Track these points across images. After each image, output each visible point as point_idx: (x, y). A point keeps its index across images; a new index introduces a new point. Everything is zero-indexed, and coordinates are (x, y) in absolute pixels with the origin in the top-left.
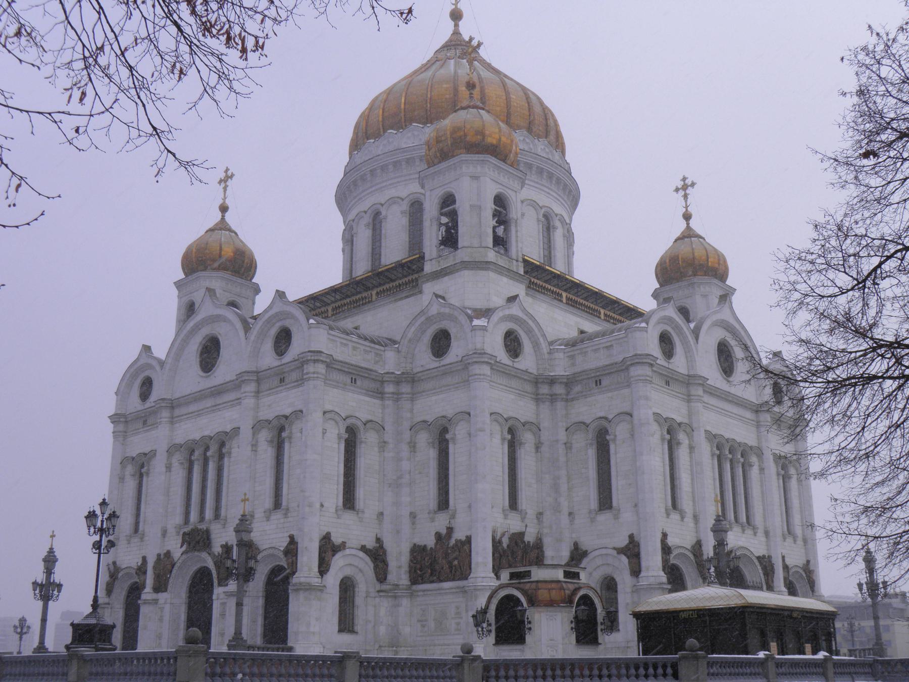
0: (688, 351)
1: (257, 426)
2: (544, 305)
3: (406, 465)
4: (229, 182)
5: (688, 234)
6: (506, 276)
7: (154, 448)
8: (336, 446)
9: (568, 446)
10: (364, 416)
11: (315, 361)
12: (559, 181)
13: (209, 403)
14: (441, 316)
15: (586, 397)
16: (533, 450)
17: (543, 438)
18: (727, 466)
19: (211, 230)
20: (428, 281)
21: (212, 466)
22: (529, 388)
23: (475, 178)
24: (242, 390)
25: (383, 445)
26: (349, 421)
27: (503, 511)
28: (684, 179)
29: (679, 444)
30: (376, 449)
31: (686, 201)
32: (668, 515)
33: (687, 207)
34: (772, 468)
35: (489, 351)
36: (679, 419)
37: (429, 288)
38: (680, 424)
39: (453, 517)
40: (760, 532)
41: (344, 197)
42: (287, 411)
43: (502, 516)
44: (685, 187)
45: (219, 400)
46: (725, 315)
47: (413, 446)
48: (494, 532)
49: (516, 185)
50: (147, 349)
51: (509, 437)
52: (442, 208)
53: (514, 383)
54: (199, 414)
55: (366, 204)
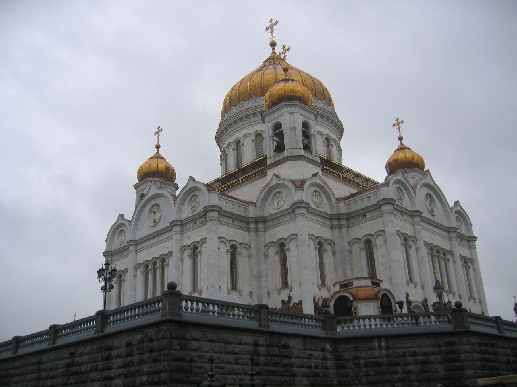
1: (183, 249)
2: (331, 180)
3: (263, 266)
4: (160, 133)
5: (402, 148)
6: (311, 163)
7: (127, 267)
8: (225, 256)
9: (350, 252)
10: (240, 241)
11: (212, 210)
12: (332, 122)
13: (155, 240)
14: (279, 186)
15: (358, 224)
16: (332, 255)
17: (337, 248)
18: (436, 260)
19: (152, 158)
20: (269, 169)
21: (158, 273)
22: (328, 222)
23: (291, 114)
24: (174, 230)
25: (250, 256)
26: (232, 243)
27: (318, 286)
28: (397, 120)
30: (247, 258)
31: (399, 131)
32: (408, 285)
34: (460, 263)
35: (305, 200)
36: (409, 234)
37: (270, 173)
38: (410, 237)
39: (291, 291)
41: (220, 138)
42: (198, 239)
43: (317, 289)
44: (398, 124)
45: (161, 238)
46: (428, 181)
47: (266, 256)
48: (314, 297)
49: (313, 117)
50: (121, 216)
51: (319, 247)
52: (274, 131)
53: (318, 219)
54: (151, 246)
55: (232, 139)
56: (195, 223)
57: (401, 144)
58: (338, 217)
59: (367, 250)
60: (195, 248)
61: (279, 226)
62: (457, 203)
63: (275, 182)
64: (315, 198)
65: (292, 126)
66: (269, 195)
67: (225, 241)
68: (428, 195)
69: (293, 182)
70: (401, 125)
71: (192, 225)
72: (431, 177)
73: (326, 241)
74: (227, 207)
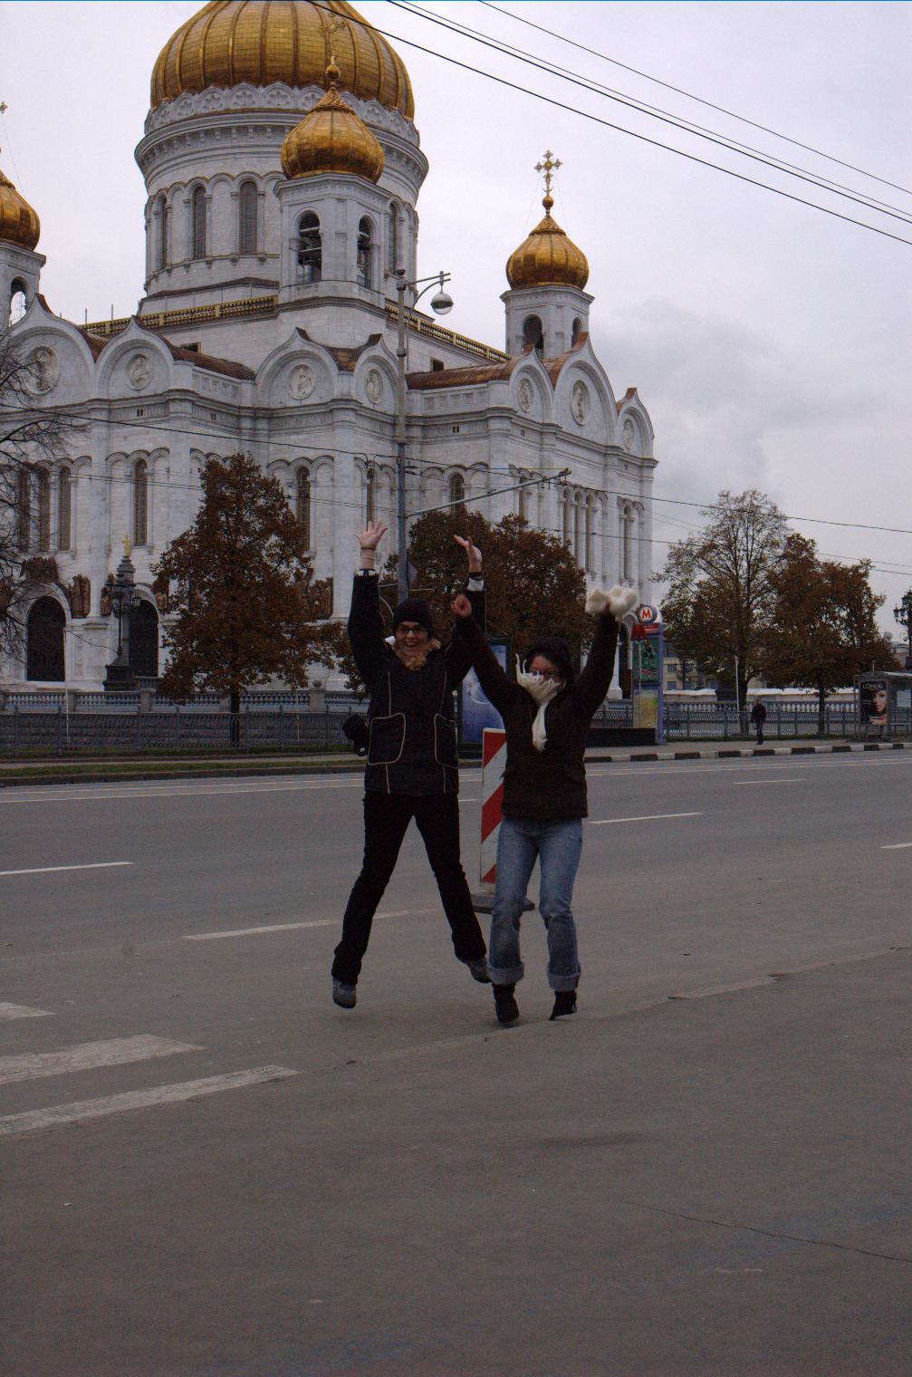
0: (544, 398)
1: (113, 459)
5: (548, 230)
6: (369, 312)
14: (306, 355)
16: (388, 493)
20: (284, 311)
22: (388, 431)
23: (340, 200)
26: (211, 458)
28: (548, 155)
29: (529, 494)
33: (548, 191)
34: (615, 512)
40: (598, 577)
42: (150, 447)
44: (548, 166)
46: (583, 355)
52: (301, 227)
56: (140, 413)
57: (548, 217)
58: (410, 421)
59: (452, 493)
60: (140, 464)
61: (298, 433)
62: (631, 392)
63: (298, 344)
64: (370, 384)
65: (341, 228)
66: (283, 367)
67: (200, 456)
68: (580, 384)
69: (333, 351)
70: (553, 171)
71: (133, 415)
72: (590, 347)
73: (381, 467)
74: (204, 388)
